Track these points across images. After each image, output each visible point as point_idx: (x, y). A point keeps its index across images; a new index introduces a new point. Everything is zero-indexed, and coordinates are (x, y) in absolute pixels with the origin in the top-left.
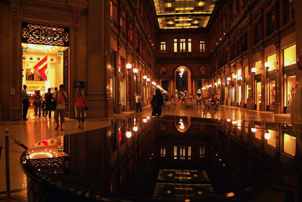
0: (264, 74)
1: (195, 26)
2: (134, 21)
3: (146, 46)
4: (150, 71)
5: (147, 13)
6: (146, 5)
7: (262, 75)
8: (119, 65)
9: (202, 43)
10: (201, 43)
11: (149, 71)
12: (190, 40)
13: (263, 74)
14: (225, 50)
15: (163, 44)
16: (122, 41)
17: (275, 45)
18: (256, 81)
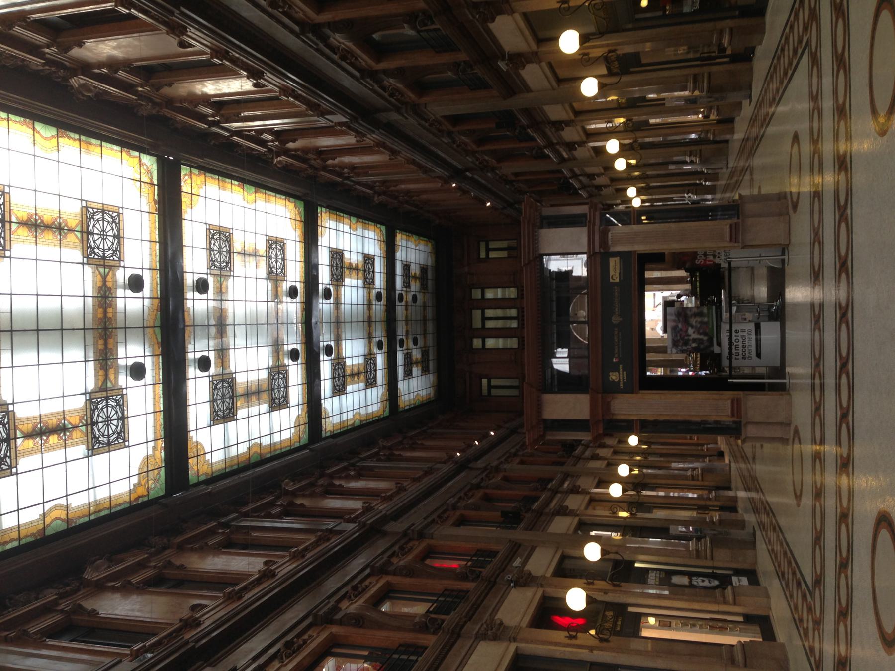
0: (608, 45)
1: (427, 279)
2: (405, 534)
3: (497, 469)
4: (587, 446)
5: (379, 460)
6: (353, 465)
7: (610, 52)
8: (573, 642)
9: (488, 250)
10: (487, 254)
11: (588, 453)
12: (477, 294)
13: (606, 49)
14: (513, 178)
15: (490, 387)
16: (469, 617)
17: (493, 20)
18: (632, 70)
